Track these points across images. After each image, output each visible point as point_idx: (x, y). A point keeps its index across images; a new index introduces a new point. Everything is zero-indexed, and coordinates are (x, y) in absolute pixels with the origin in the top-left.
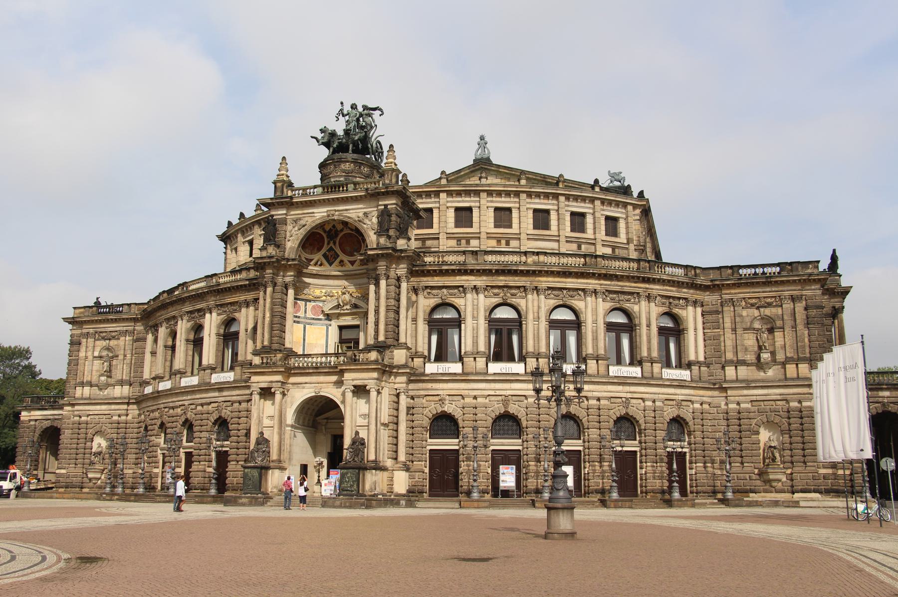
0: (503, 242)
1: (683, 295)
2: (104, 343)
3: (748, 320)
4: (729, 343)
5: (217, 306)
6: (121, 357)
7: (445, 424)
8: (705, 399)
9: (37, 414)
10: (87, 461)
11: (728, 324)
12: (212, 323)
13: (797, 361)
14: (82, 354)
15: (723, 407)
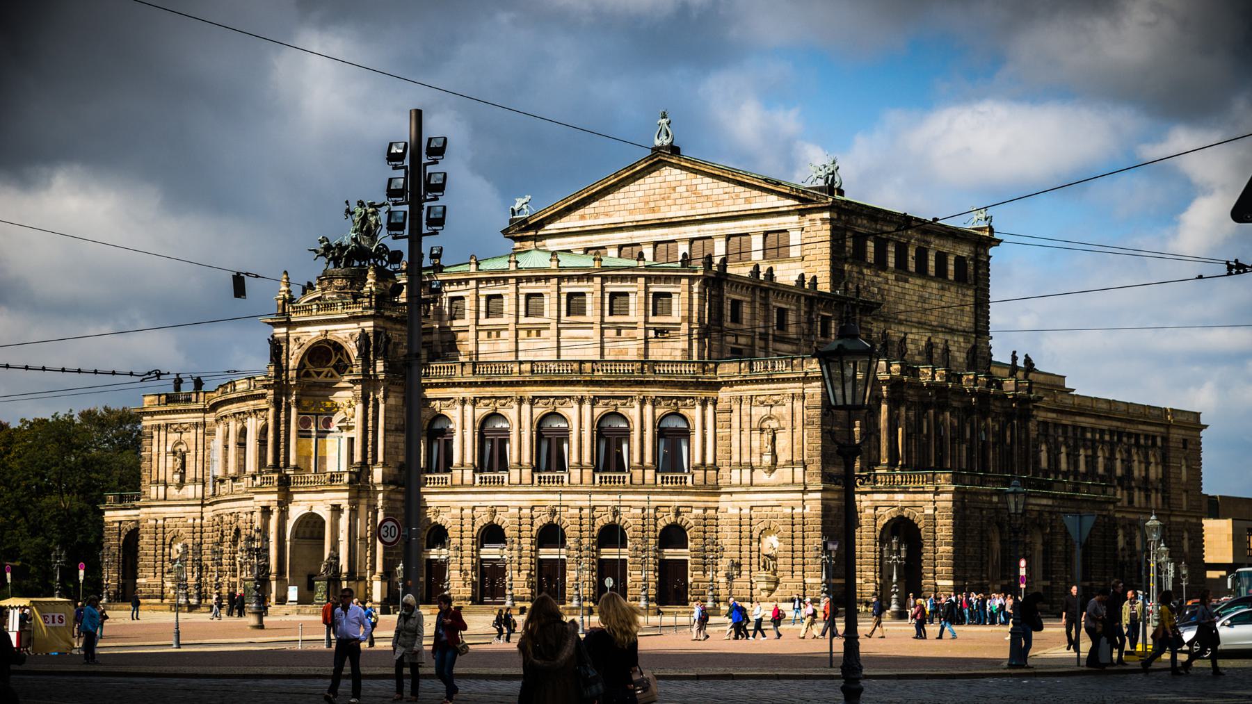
0: (534, 332)
1: (688, 394)
2: (176, 436)
3: (755, 420)
4: (735, 444)
5: (255, 411)
6: (193, 453)
7: (439, 535)
8: (710, 504)
9: (121, 515)
10: (166, 569)
11: (736, 424)
12: (253, 425)
13: (792, 463)
14: (155, 449)
15: (731, 511)
